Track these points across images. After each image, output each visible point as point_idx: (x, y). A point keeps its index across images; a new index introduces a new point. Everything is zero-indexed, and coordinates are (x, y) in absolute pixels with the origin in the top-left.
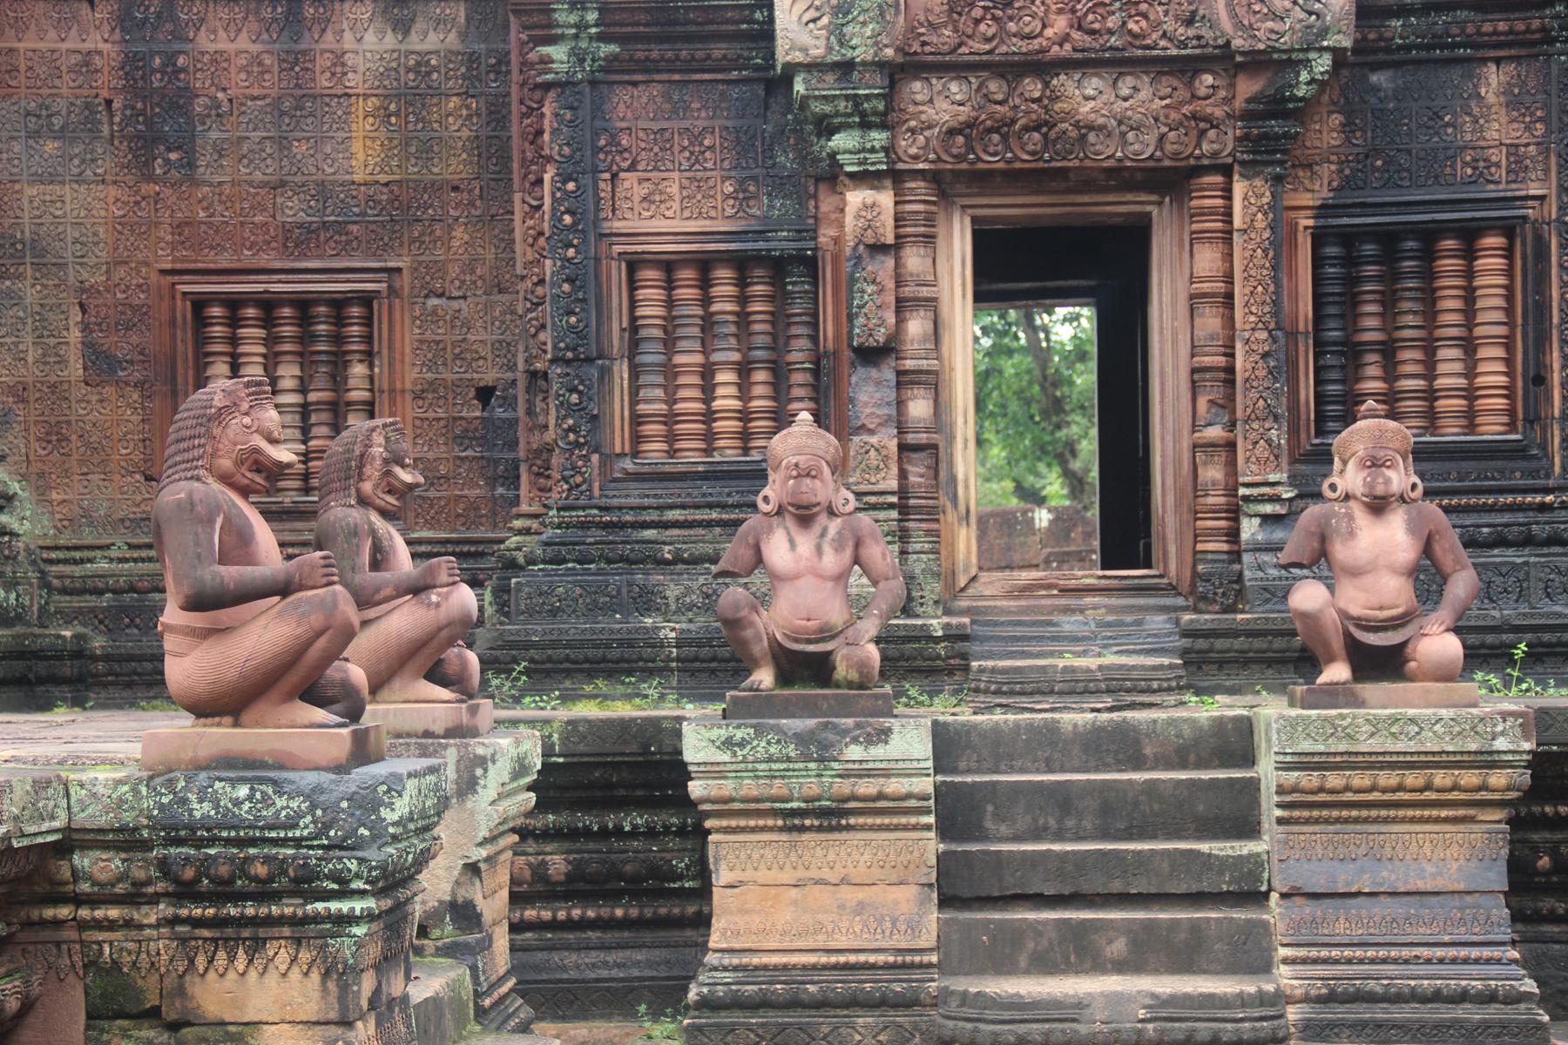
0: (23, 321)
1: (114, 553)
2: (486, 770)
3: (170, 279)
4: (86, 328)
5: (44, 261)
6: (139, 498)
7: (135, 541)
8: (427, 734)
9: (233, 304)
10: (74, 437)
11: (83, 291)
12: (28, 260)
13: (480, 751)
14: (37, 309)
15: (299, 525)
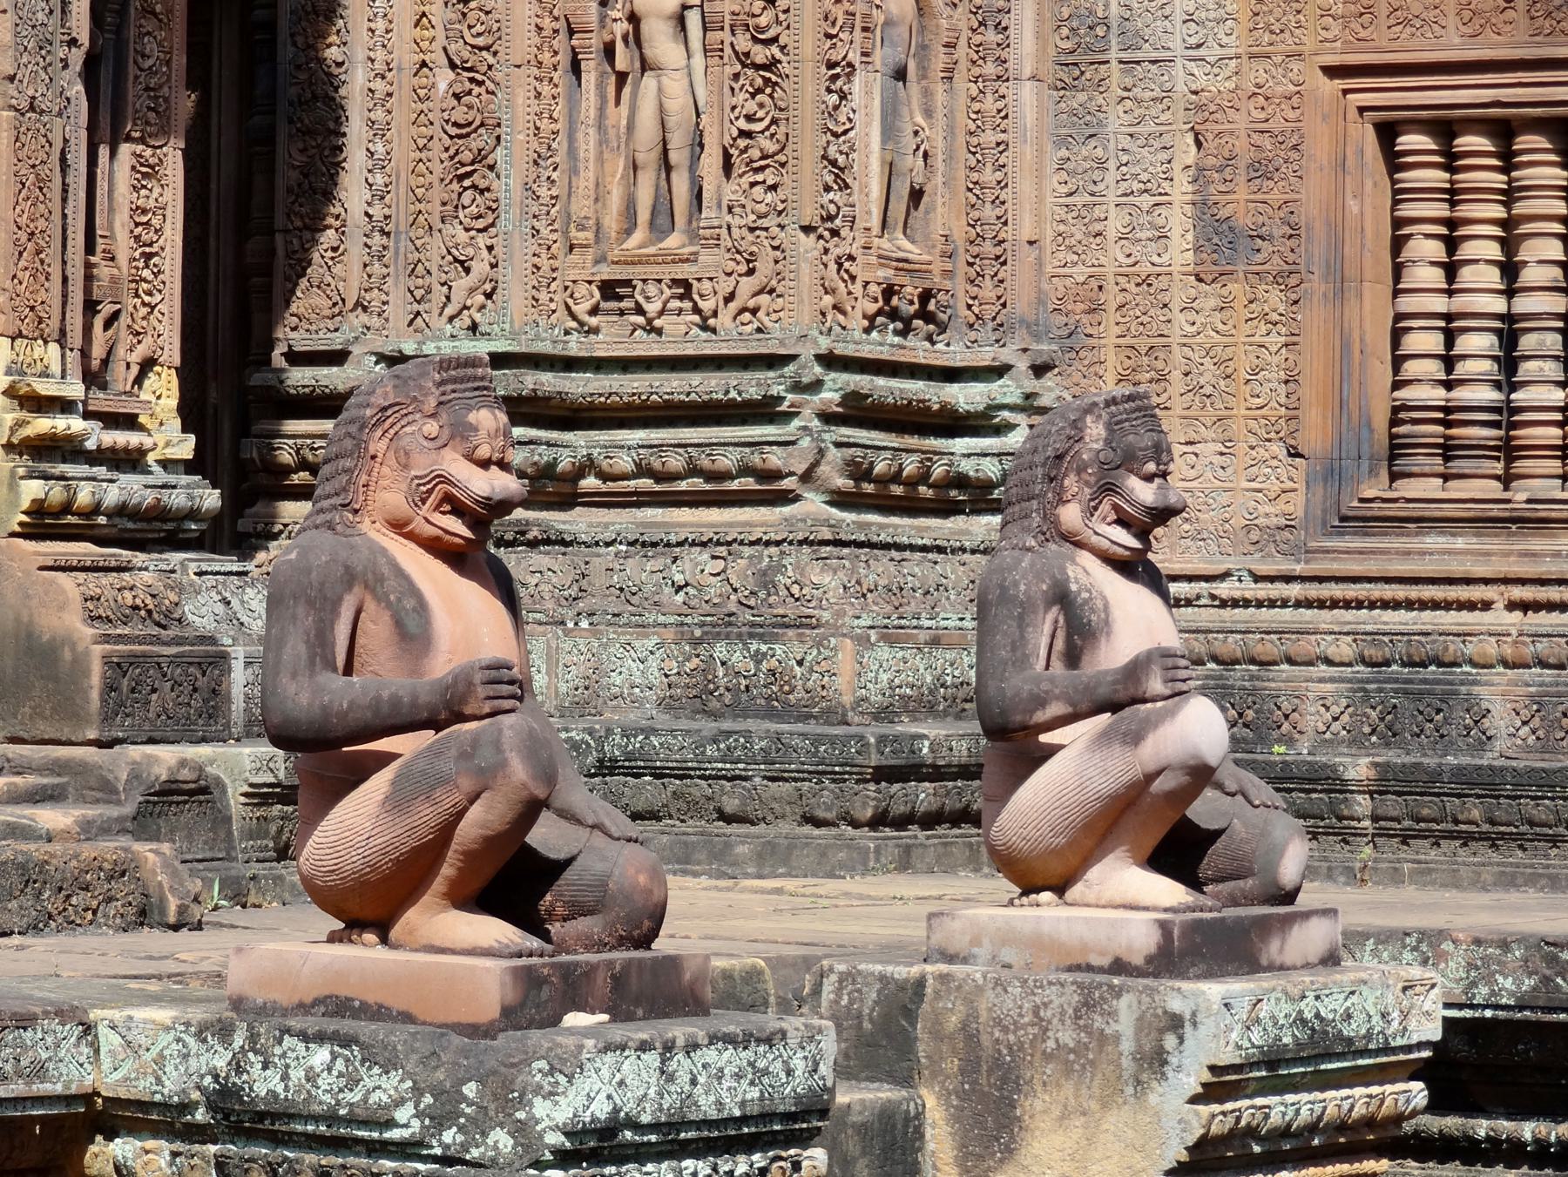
0: (1101, 164)
1: (1224, 589)
2: (1181, 1040)
3: (1340, 84)
4: (1199, 175)
5: (1139, 55)
6: (1276, 487)
7: (1264, 568)
8: (1119, 967)
9: (1445, 128)
10: (1176, 375)
11: (1200, 108)
12: (1114, 54)
13: (1176, 1005)
14: (1126, 142)
15: (1537, 544)
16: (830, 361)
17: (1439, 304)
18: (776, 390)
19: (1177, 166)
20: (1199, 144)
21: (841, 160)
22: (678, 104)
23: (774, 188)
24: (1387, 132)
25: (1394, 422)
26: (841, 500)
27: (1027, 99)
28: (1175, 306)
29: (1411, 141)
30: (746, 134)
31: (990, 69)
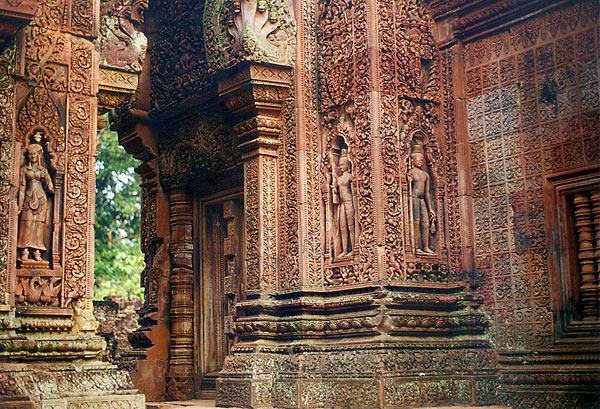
11: (513, 198)
16: (389, 288)
17: (590, 255)
18: (370, 298)
19: (508, 217)
20: (514, 210)
21: (395, 224)
22: (349, 212)
23: (372, 233)
24: (570, 197)
25: (581, 298)
26: (394, 333)
27: (463, 200)
28: (511, 263)
29: (577, 200)
30: (364, 218)
31: (453, 194)
